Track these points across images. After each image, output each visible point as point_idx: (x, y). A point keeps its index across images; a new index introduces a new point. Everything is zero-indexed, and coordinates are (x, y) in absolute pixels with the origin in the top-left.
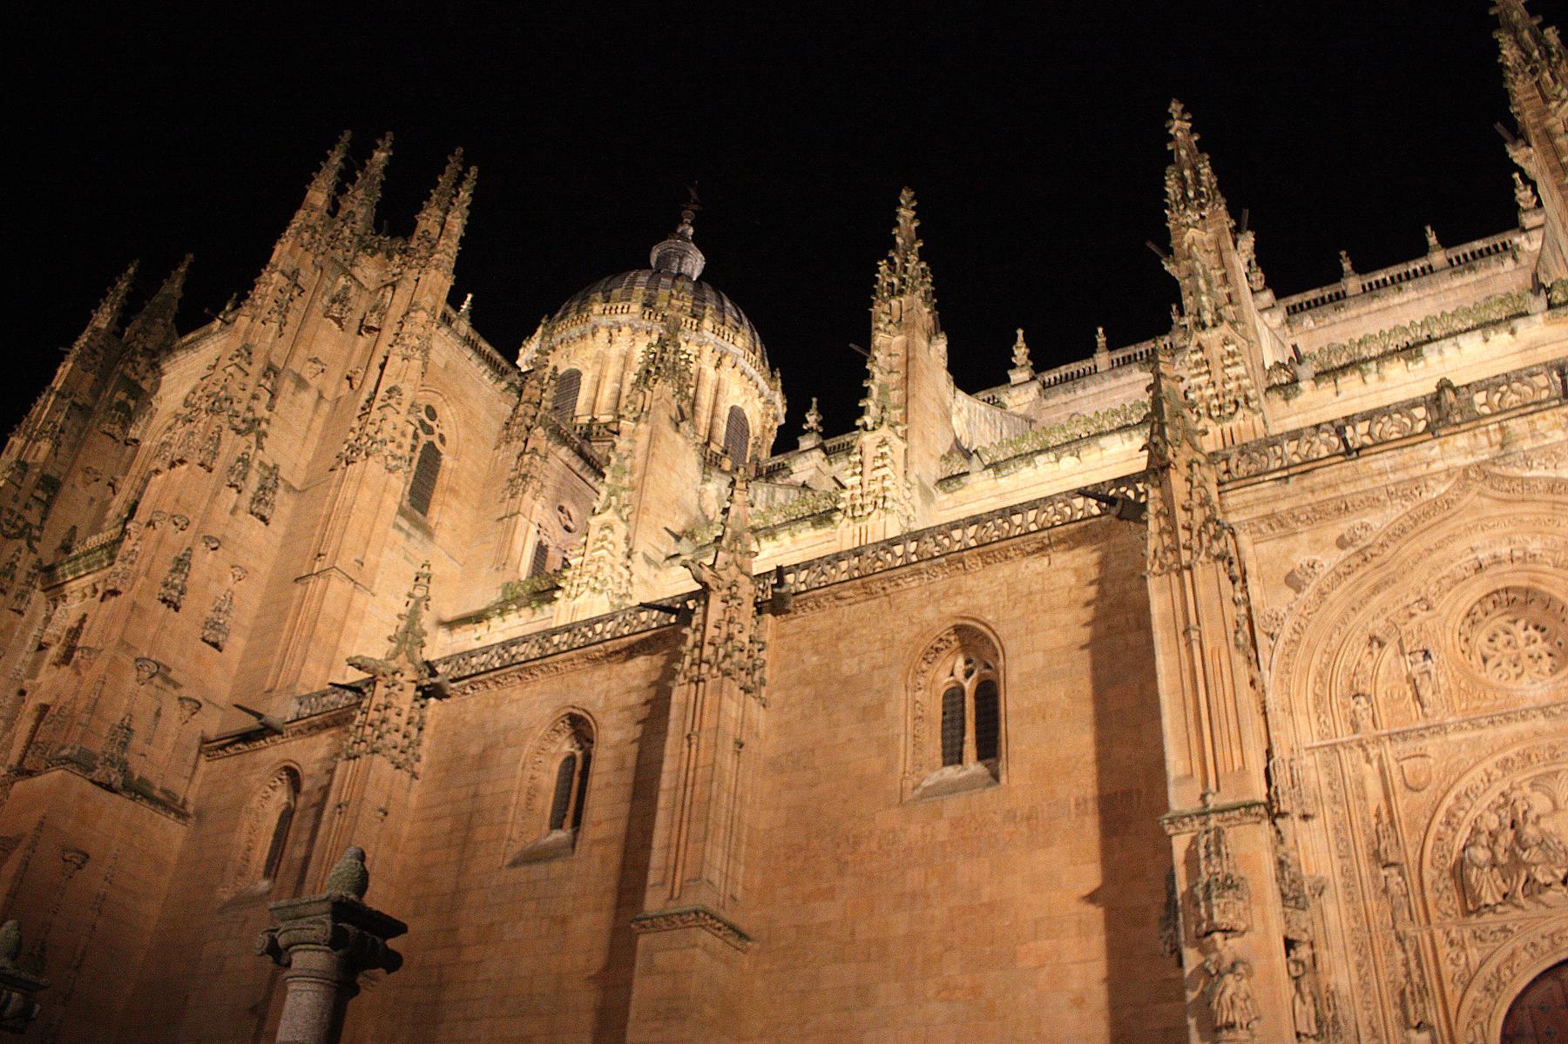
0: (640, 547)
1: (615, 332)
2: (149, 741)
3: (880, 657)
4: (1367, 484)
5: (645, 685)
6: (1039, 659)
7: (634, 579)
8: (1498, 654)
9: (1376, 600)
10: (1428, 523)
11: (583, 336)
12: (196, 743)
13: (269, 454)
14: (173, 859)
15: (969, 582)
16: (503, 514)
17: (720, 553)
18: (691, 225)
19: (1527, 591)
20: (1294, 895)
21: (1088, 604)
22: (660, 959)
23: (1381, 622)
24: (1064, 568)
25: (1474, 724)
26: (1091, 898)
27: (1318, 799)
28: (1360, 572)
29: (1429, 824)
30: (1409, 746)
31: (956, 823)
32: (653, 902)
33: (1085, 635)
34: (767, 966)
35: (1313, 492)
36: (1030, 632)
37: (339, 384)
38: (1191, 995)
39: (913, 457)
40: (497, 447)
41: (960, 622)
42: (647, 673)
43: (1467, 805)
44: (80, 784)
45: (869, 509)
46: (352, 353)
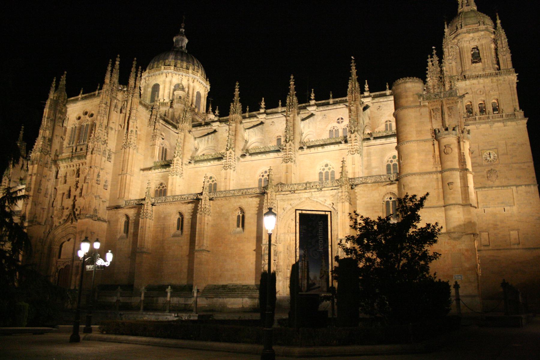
0: (184, 163)
1: (167, 74)
2: (99, 210)
5: (191, 209)
7: (183, 170)
11: (159, 74)
12: (106, 208)
14: (106, 230)
15: (241, 200)
16: (151, 144)
18: (184, 28)
21: (257, 207)
22: (198, 256)
26: (254, 250)
27: (282, 241)
32: (197, 248)
33: (256, 212)
36: (249, 210)
37: (118, 126)
38: (263, 266)
39: (236, 153)
42: (192, 207)
44: (91, 220)
45: (228, 168)
46: (120, 118)
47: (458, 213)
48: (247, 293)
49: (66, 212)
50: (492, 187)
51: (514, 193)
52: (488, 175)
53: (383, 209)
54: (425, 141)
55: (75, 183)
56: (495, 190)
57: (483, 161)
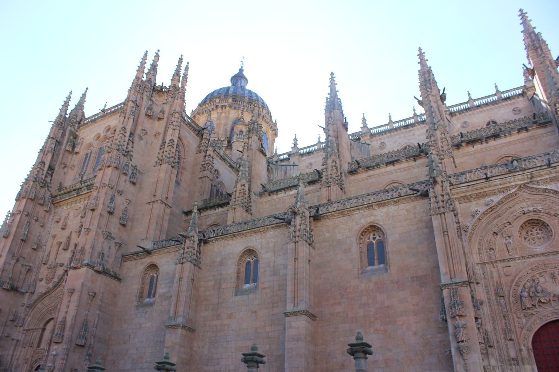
2: (108, 257)
4: (493, 188)
6: (397, 236)
8: (529, 237)
9: (495, 222)
10: (510, 200)
13: (134, 162)
15: (375, 212)
16: (201, 176)
17: (298, 203)
19: (538, 220)
20: (477, 304)
22: (293, 324)
23: (496, 228)
24: (403, 209)
25: (523, 258)
28: (491, 213)
29: (511, 286)
30: (506, 264)
31: (376, 284)
34: (322, 325)
35: (477, 190)
40: (197, 154)
41: (372, 224)
43: (521, 280)
49: (60, 271)
55: (80, 225)
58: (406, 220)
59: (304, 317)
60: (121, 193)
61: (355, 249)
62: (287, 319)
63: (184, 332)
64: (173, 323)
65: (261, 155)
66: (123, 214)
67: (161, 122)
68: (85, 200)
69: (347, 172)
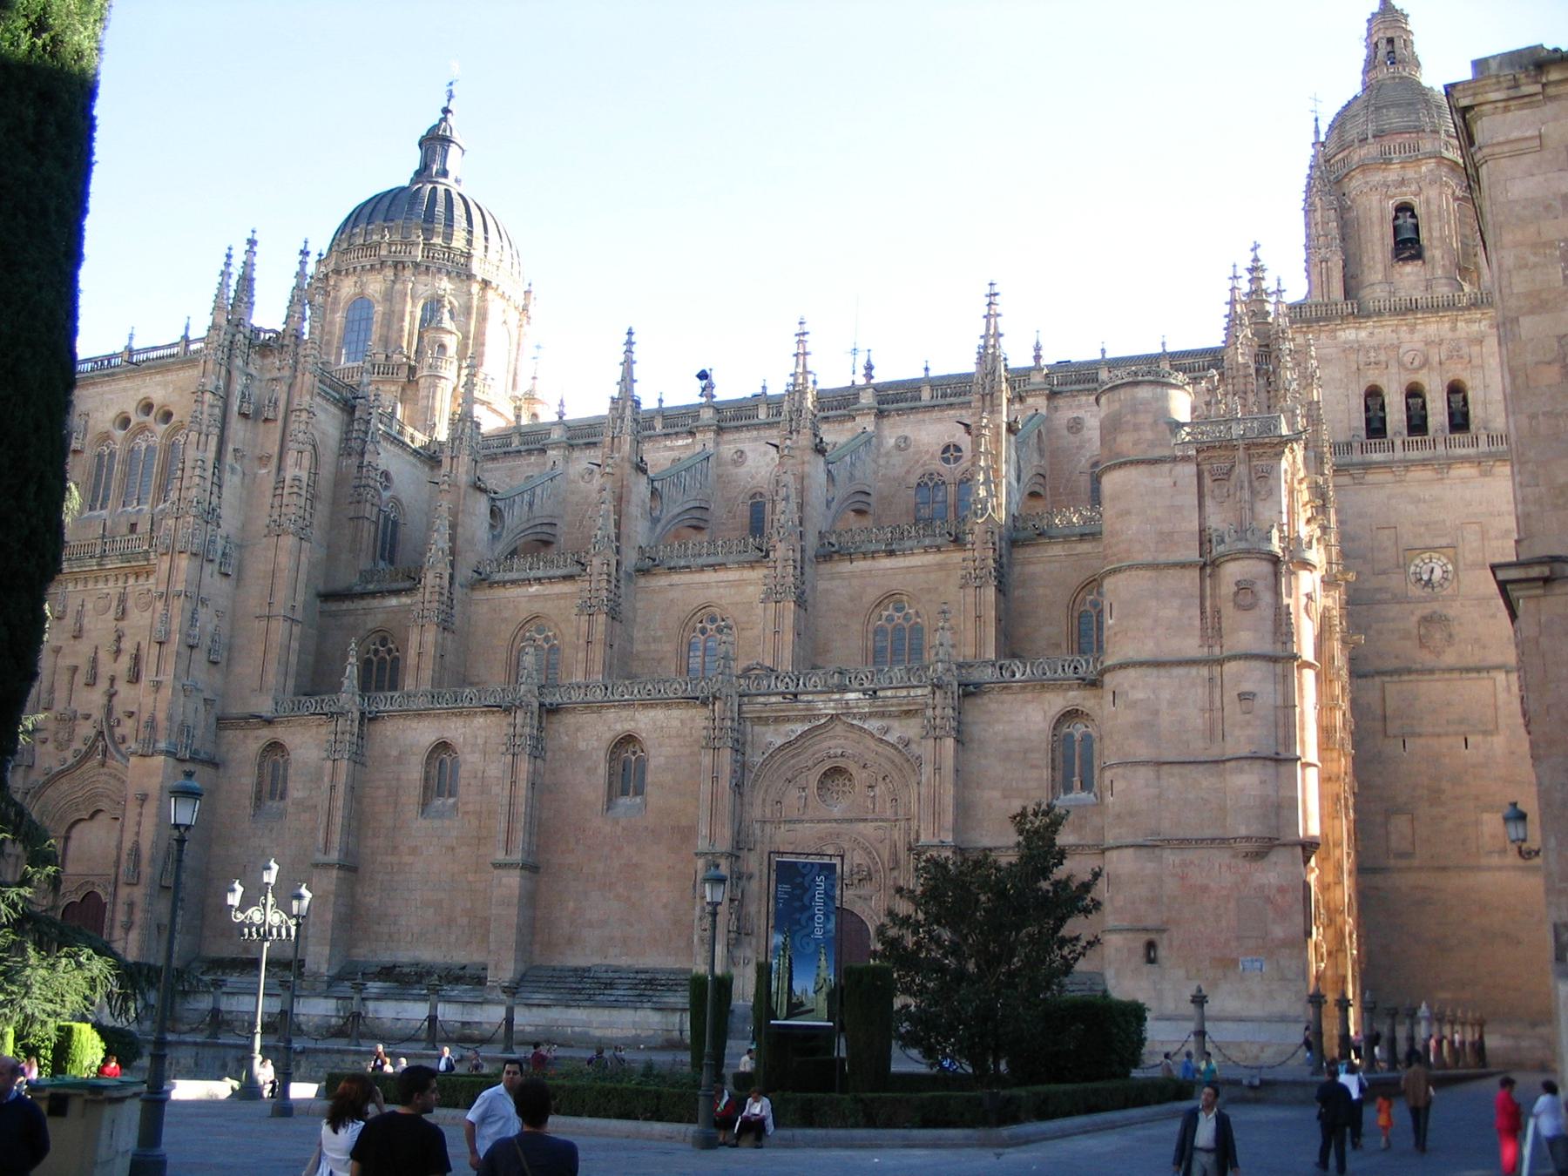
3: (596, 744)
6: (662, 760)
16: (352, 514)
30: (792, 826)
47: (1263, 782)
48: (651, 993)
49: (86, 730)
50: (1431, 671)
51: (1499, 689)
52: (1422, 631)
53: (1053, 760)
54: (1183, 565)
55: (114, 637)
56: (1438, 680)
57: (1410, 585)
58: (678, 736)
59: (518, 872)
60: (203, 602)
61: (603, 770)
62: (496, 872)
63: (342, 874)
64: (320, 858)
65: (478, 494)
66: (213, 641)
67: (272, 425)
68: (117, 579)
69: (632, 570)
